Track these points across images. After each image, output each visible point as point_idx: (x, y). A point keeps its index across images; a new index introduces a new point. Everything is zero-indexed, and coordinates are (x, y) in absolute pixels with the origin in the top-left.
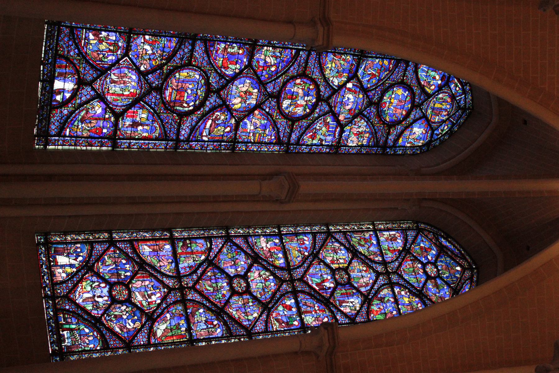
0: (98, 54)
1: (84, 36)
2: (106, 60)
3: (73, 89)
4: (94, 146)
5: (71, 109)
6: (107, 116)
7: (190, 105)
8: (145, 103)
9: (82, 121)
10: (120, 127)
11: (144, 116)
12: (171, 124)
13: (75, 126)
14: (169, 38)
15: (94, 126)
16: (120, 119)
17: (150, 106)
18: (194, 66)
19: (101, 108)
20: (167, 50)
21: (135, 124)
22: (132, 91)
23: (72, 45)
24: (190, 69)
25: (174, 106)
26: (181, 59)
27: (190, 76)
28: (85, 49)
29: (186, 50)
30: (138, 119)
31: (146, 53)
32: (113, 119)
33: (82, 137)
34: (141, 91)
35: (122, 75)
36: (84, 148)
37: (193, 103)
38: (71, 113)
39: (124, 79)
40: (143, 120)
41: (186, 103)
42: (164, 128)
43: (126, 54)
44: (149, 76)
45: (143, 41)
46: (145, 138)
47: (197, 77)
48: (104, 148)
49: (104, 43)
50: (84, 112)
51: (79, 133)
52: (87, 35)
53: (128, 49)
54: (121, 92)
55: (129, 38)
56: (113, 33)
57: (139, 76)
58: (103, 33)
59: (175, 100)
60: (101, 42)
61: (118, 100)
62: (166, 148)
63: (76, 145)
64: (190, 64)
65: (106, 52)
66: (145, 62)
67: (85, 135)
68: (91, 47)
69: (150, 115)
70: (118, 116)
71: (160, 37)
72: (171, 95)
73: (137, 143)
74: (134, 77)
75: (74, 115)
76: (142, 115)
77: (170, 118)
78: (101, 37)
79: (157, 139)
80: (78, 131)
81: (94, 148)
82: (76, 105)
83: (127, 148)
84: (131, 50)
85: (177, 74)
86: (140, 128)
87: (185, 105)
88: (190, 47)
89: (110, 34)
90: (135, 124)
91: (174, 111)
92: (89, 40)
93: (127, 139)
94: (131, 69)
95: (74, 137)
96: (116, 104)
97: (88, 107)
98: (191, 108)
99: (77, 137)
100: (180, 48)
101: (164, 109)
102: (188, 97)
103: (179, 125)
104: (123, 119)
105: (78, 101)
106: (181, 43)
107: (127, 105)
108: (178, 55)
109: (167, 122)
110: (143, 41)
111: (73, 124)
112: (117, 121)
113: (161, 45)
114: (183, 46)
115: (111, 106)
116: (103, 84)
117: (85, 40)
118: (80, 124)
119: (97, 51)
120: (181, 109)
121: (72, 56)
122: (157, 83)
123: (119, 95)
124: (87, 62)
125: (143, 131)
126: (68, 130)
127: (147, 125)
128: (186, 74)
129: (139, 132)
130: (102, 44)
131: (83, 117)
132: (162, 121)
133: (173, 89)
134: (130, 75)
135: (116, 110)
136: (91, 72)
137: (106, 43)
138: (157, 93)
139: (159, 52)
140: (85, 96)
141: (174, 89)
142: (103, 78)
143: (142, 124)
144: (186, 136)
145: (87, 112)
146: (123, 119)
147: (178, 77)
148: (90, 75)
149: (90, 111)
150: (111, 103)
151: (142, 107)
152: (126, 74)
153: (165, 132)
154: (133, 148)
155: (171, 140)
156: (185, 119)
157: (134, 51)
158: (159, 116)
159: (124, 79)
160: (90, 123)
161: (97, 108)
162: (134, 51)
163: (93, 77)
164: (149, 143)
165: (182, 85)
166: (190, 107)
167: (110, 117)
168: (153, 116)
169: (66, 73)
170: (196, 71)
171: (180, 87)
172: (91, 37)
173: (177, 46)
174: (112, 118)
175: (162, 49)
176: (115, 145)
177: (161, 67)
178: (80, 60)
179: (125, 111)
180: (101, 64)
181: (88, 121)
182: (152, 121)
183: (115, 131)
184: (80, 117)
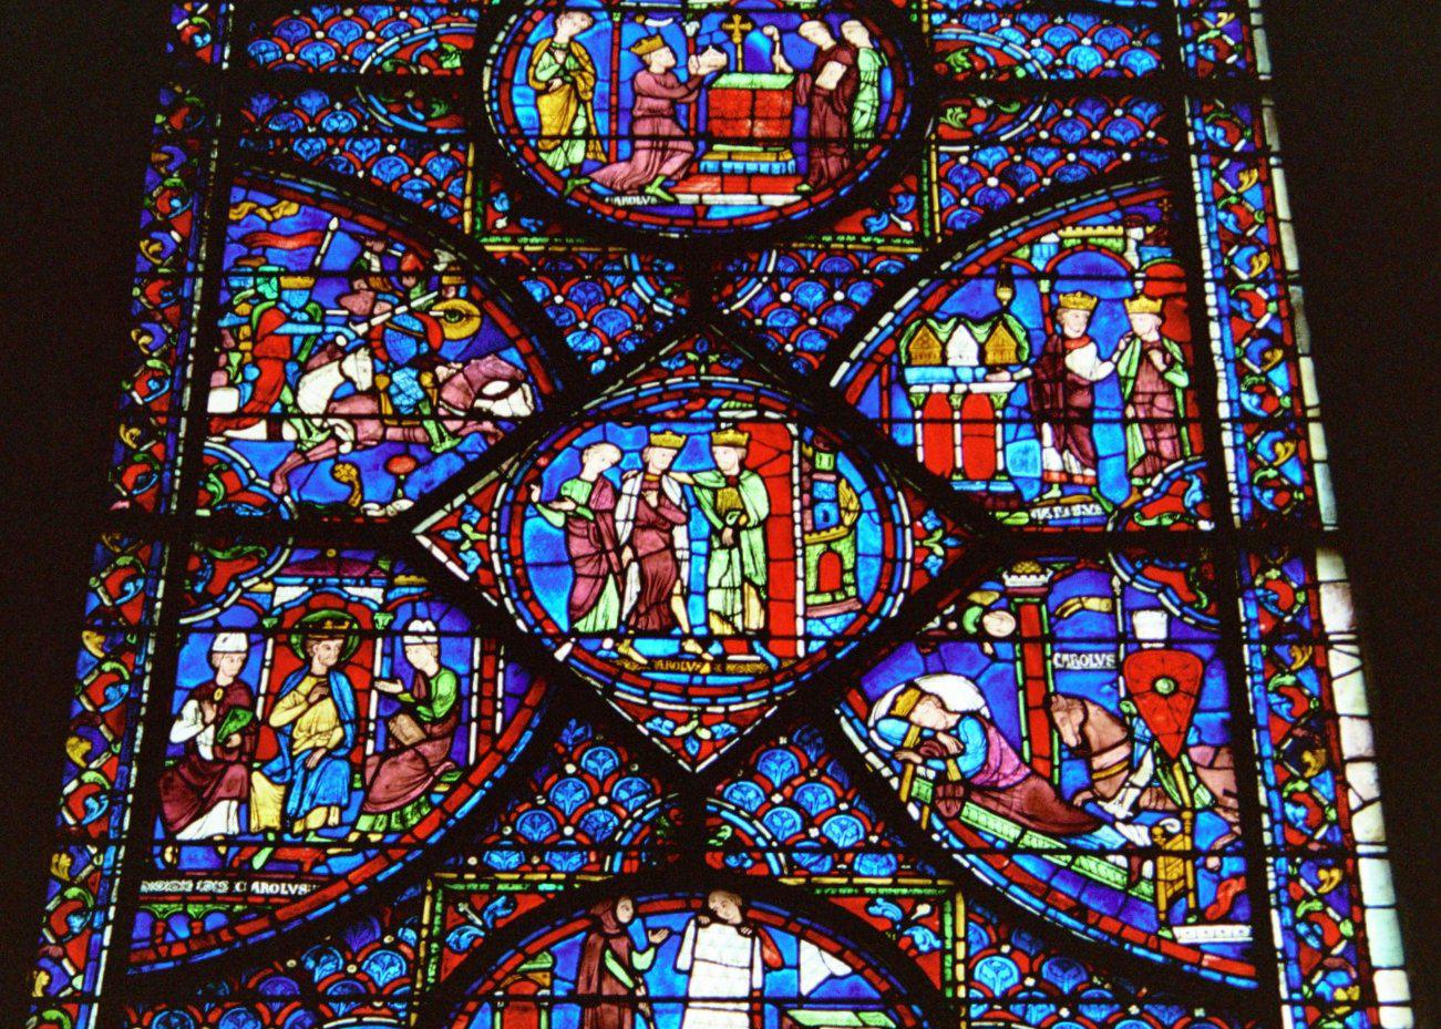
0: (384, 755)
1: (209, 886)
2: (445, 686)
3: (752, 926)
4: (1327, 697)
5: (958, 919)
6: (1001, 624)
7: (824, 40)
8: (837, 349)
9: (1075, 821)
10: (1093, 511)
11: (963, 347)
12: (1017, 144)
13: (1134, 877)
14: (233, 251)
15: (1118, 718)
16: (1021, 518)
17: (865, 318)
18: (474, 61)
19: (928, 684)
20: (337, 250)
21: (1054, 401)
22: (729, 459)
23: (303, 975)
24: (504, 82)
25: (848, 137)
26: (419, 148)
27: (564, 71)
28: (339, 865)
29: (340, 123)
30: (1000, 386)
31: (373, 393)
32: (1024, 579)
33: (1250, 811)
34: (732, 394)
35: (579, 546)
36: (1363, 779)
37: (816, 33)
38: (1002, 920)
39: (624, 531)
40: (1004, 346)
41: (815, 70)
42: (1060, 191)
43: (390, 544)
44: (591, 344)
45: (259, 431)
46: (1185, 317)
47: (570, 25)
48: (1336, 613)
49: (279, 718)
50: (973, 813)
51: (1211, 831)
52: (201, 858)
53: (334, 537)
54: (754, 539)
55: (226, 528)
56: (191, 650)
57: (599, 417)
58: (180, 733)
59: (786, 142)
60: (262, 746)
61: (830, 554)
62: (1254, 158)
63: (1343, 853)
64: (460, 91)
65: (361, 695)
66: (450, 394)
67: (1220, 780)
68: (316, 819)
69: (951, 306)
70: (985, 538)
71: (215, 307)
72: (749, 182)
73: (1241, 373)
74: (600, 459)
75: (1018, 895)
76: (960, 357)
77: (966, 161)
78: (220, 744)
79: (1177, 235)
80: (1182, 844)
81: (1349, 695)
82: (918, 885)
83: (1302, 438)
84: (341, 509)
85: (556, 160)
86: (1084, 362)
87: (831, 76)
88: (312, 102)
89: (188, 681)
90: (1054, 401)
91: (902, 147)
92: (245, 840)
93: (1214, 452)
94: (520, 489)
95: (1255, 874)
96: (871, 571)
97: (924, 789)
98: (856, 33)
99: (1249, 847)
100: (320, 168)
101: (886, 206)
102: (755, 62)
103: (1032, 90)
104: (1016, 501)
105: (874, 871)
106: (270, 169)
107: (873, 485)
108: (387, 172)
109: (1007, 174)
110: (259, 431)
111: (1122, 902)
112: (1039, 544)
113: (298, 300)
114: (307, 148)
115: (892, 607)
116: (685, 692)
117: (251, 875)
118: (1105, 835)
119: (358, 768)
120: (867, 98)
121: (415, 965)
122: (642, 289)
123: (781, 555)
124: (472, 835)
125: (1108, 333)
126: (1186, 935)
127: (1051, 313)
128: (546, 102)
129: (1127, 363)
130: (286, 731)
131: (1031, 818)
132: (996, 215)
133: (691, 170)
134: (578, 491)
135: (934, 564)
136: (569, 798)
137: (274, 697)
138: (735, 281)
139: (358, 304)
140: (809, 821)
141: (694, 160)
142: (624, 692)
143: (1049, 355)
144: (1112, 41)
145: (980, 788)
146: (1016, 501)
147: (577, 153)
148: (597, 796)
149: (969, 763)
150: (866, 610)
151: (888, 369)
152: (572, 518)
153: (1096, 179)
154: (1296, 391)
155: (1173, 127)
156: (959, 59)
157: (356, 485)
158: (956, 240)
159: (624, 531)
160: (1084, 752)
161: (927, 715)
162: (356, 485)
163: (621, 771)
164: (1227, 281)
165: (654, 114)
166: (842, 43)
167: (1010, 601)
168: (960, 278)
169: (588, 1002)
170: (519, 40)
171: (666, 127)
172: (219, 821)
173: (308, 185)
174: (1011, 581)
175: (334, 289)
176: (1288, 534)
177: (493, 283)
178: (452, 899)
179: (932, 490)
180: (485, 719)
181: (1074, 775)
182: (1006, 279)
183: (1150, 549)
184: (1035, 840)
